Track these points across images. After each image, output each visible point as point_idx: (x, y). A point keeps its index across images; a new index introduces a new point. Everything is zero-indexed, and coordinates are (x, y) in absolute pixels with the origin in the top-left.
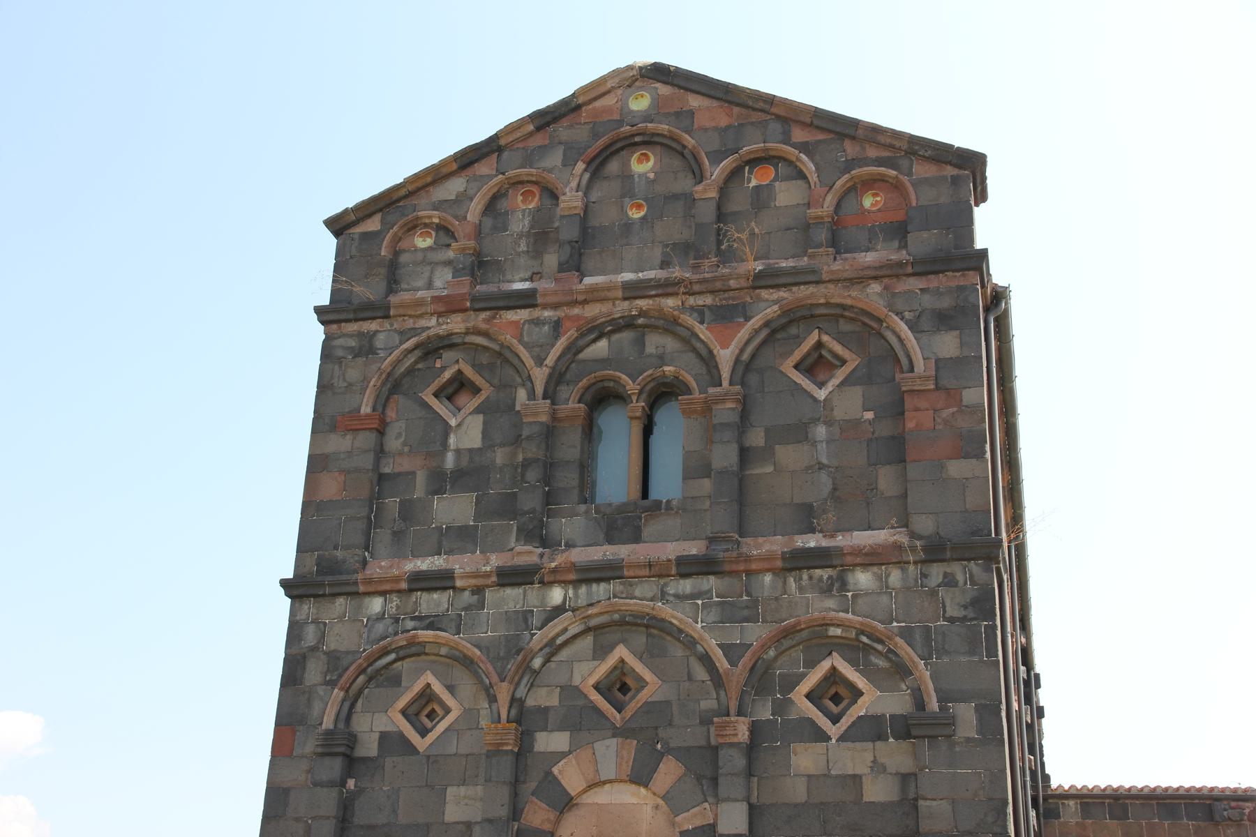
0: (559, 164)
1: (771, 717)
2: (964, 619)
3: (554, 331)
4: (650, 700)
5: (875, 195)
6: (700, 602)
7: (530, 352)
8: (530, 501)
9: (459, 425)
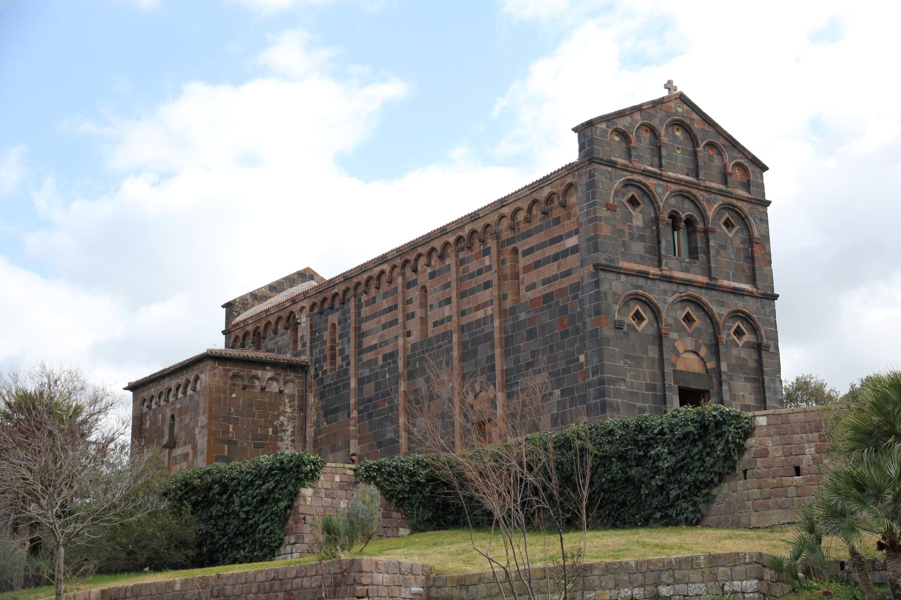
5: (738, 169)
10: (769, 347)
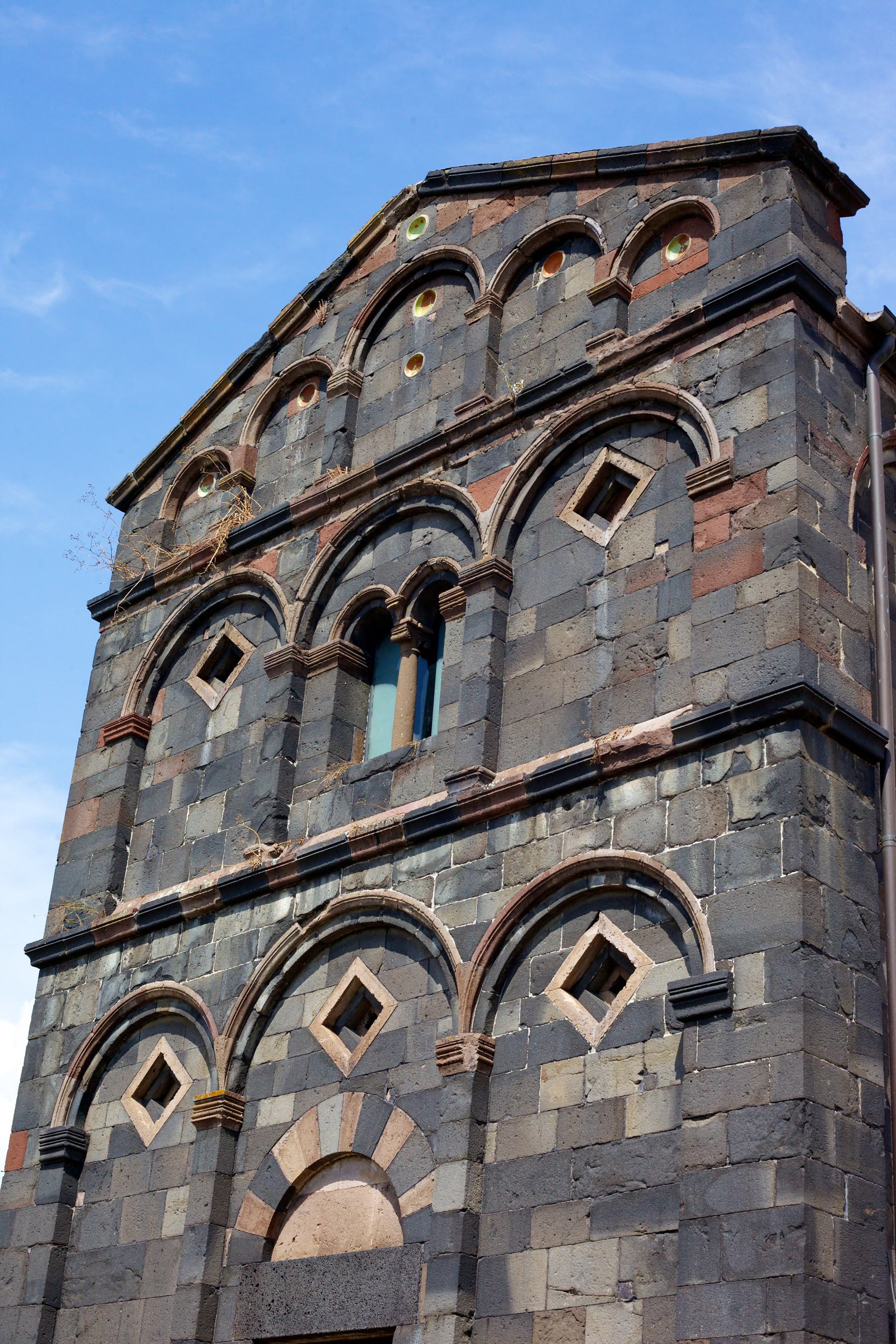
0: (332, 341)
1: (520, 1029)
2: (756, 820)
3: (309, 551)
4: (383, 1031)
6: (435, 876)
7: (283, 588)
8: (269, 784)
9: (218, 706)
10: (723, 994)
